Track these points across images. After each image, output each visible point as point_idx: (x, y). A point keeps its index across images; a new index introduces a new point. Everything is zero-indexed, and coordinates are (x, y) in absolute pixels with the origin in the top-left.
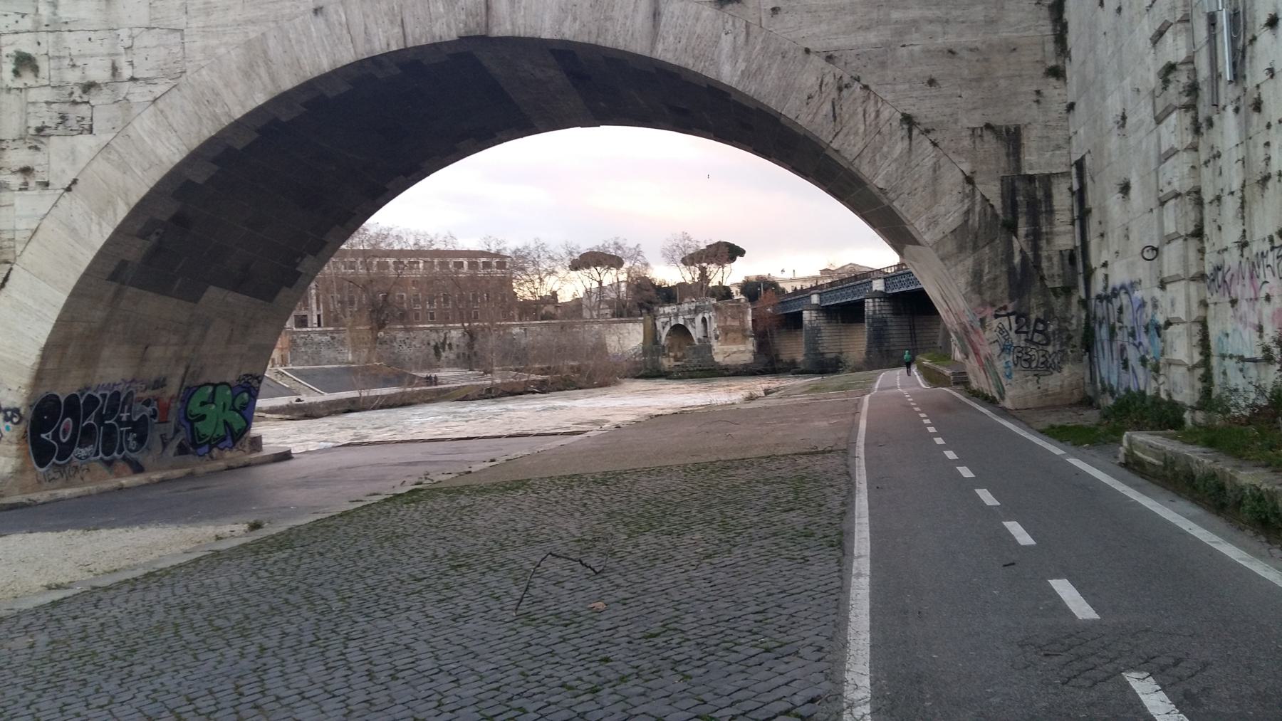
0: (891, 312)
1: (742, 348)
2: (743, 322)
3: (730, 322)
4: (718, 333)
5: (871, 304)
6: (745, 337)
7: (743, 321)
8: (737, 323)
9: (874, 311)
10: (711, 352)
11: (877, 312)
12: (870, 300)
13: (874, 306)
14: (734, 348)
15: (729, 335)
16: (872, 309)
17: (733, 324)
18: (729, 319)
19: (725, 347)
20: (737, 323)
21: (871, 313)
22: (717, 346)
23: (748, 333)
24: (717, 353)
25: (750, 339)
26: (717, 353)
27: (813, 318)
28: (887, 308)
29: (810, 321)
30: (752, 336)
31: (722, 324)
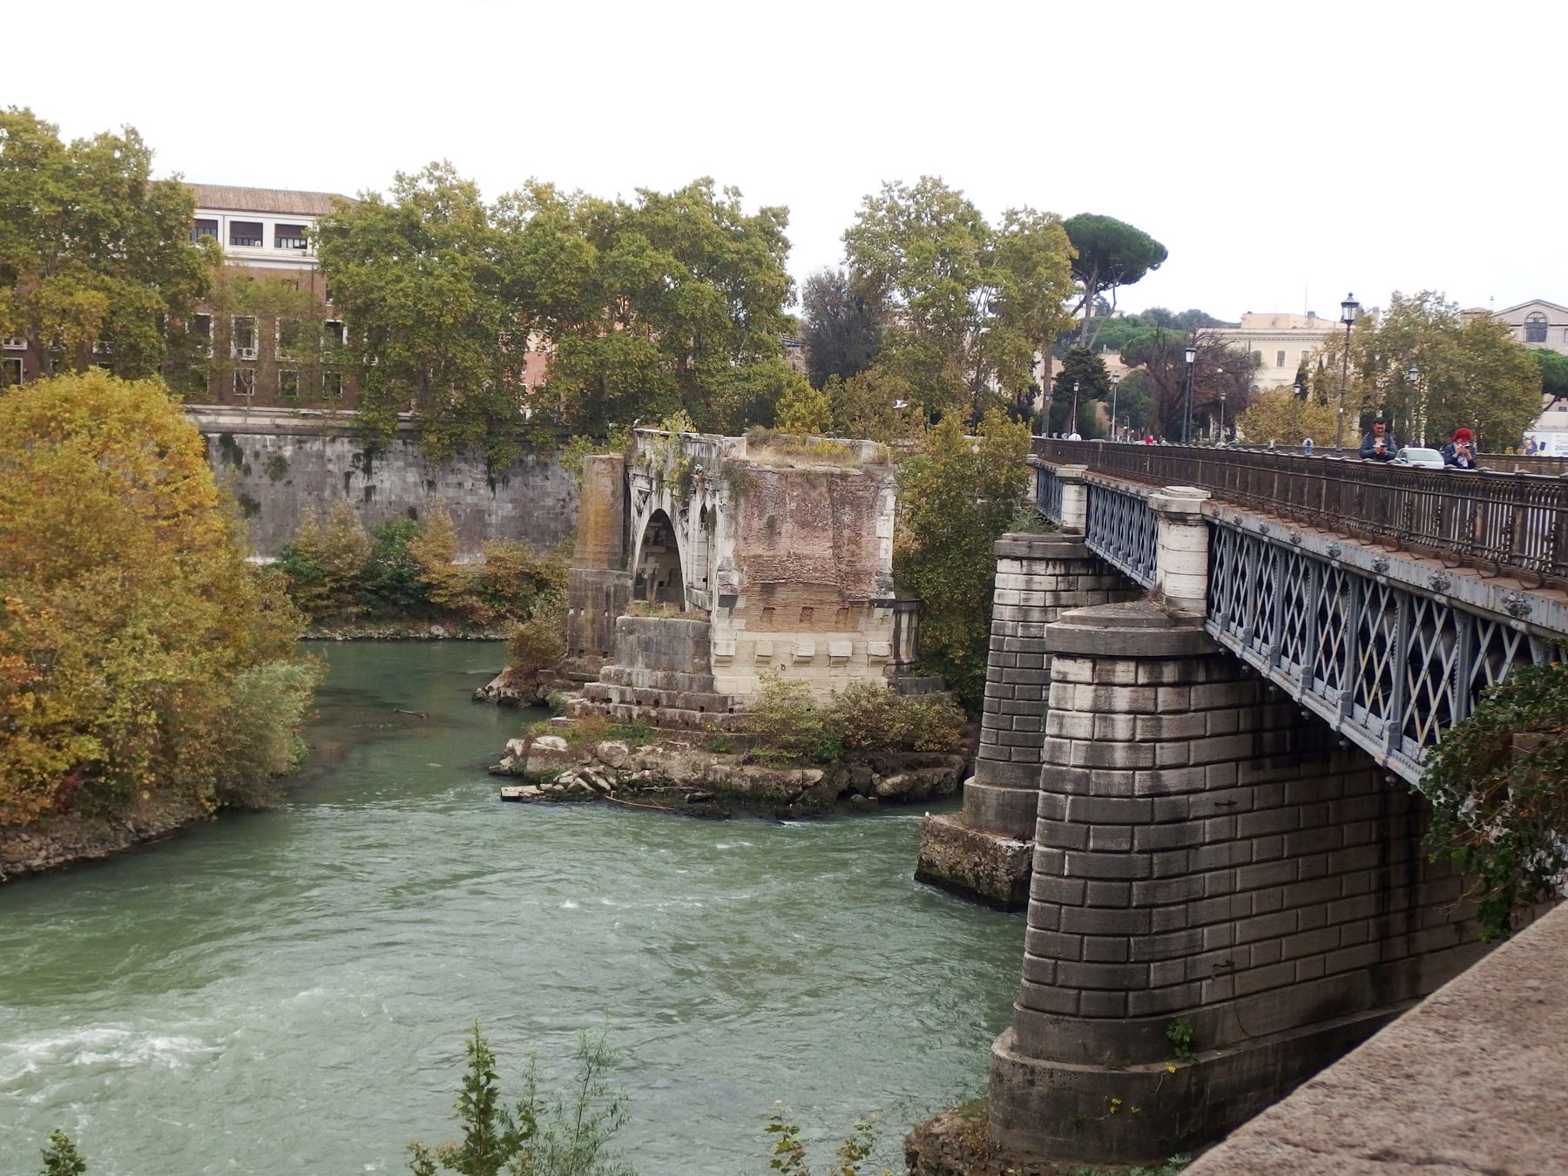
0: (1225, 747)
1: (840, 644)
2: (850, 542)
3: (789, 541)
4: (735, 579)
5: (1084, 697)
6: (852, 609)
7: (856, 540)
8: (819, 548)
9: (1099, 747)
10: (708, 654)
11: (1120, 755)
12: (1081, 670)
13: (1101, 712)
14: (806, 642)
15: (781, 595)
16: (1081, 726)
17: (803, 549)
18: (787, 527)
19: (766, 640)
20: (819, 548)
21: (1074, 756)
22: (727, 635)
23: (872, 591)
24: (726, 661)
25: (879, 612)
26: (726, 661)
27: (1037, 599)
28: (1212, 722)
29: (1024, 610)
30: (881, 603)
31: (758, 549)
